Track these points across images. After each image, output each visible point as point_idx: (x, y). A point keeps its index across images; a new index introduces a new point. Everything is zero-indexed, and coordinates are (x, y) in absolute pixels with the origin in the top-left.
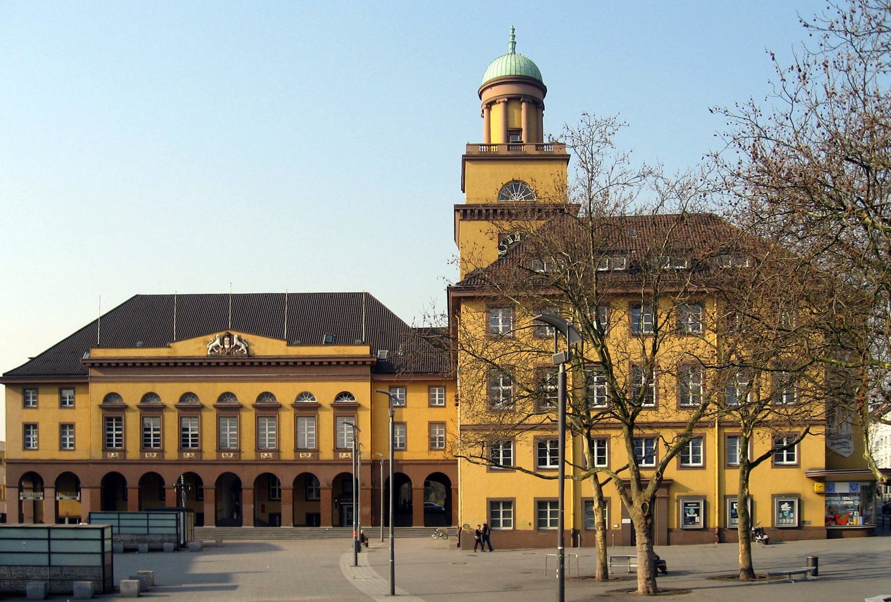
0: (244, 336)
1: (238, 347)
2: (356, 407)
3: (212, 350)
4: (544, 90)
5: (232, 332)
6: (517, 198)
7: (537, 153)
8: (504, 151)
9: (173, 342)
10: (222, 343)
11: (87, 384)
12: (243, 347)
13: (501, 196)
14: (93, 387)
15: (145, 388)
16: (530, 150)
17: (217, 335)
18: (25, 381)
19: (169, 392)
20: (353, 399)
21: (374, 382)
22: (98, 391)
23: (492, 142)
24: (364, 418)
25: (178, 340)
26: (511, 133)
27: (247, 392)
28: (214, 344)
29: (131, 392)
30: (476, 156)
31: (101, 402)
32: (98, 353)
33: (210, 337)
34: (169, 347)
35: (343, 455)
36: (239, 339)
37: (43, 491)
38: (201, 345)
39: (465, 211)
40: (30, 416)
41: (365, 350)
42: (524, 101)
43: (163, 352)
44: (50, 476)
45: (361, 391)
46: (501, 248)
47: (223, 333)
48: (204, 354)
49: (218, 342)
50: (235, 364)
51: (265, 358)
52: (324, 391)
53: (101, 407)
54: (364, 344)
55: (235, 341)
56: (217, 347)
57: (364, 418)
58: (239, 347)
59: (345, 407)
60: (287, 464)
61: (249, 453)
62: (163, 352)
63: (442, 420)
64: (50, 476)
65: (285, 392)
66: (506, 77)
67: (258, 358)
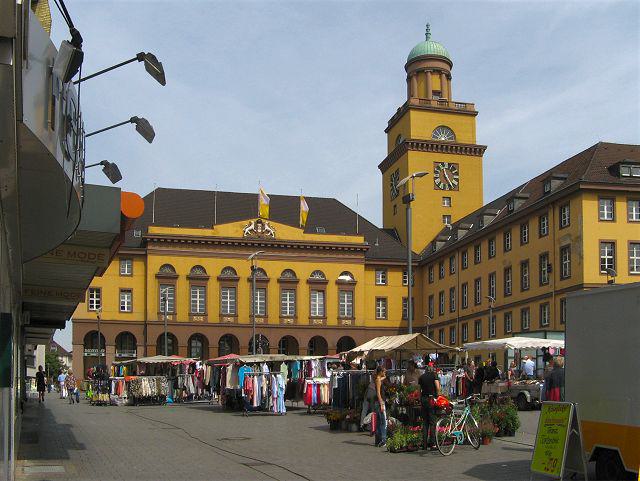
10: (256, 227)
11: (146, 256)
14: (151, 258)
15: (196, 261)
19: (214, 266)
21: (366, 265)
22: (155, 262)
25: (219, 223)
27: (274, 268)
29: (183, 265)
32: (154, 230)
33: (246, 223)
35: (226, 319)
41: (360, 240)
43: (208, 233)
44: (111, 335)
45: (358, 269)
47: (256, 220)
48: (240, 236)
49: (252, 227)
51: (289, 241)
52: (333, 271)
53: (157, 277)
54: (359, 234)
55: (267, 228)
62: (208, 233)
64: (111, 335)
65: (304, 270)
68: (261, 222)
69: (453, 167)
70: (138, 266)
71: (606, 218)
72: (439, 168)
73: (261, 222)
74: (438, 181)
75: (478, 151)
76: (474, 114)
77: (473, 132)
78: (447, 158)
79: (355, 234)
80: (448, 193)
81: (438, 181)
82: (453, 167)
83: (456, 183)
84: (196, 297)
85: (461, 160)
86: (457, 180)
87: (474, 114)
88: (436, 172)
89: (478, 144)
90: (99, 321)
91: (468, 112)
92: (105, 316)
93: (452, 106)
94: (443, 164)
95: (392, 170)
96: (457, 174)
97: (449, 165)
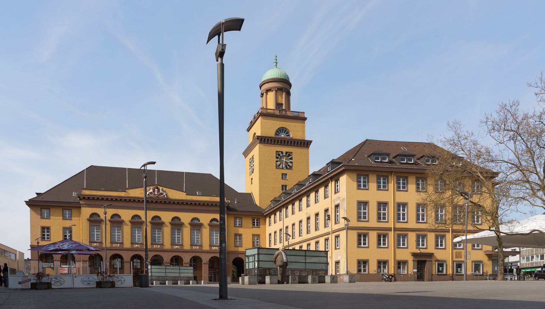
0: (165, 189)
1: (162, 194)
5: (159, 187)
9: (128, 189)
10: (154, 191)
11: (80, 207)
12: (165, 194)
13: (276, 134)
18: (38, 204)
20: (199, 221)
29: (106, 213)
30: (264, 114)
31: (88, 217)
34: (125, 192)
36: (163, 191)
37: (53, 262)
39: (261, 139)
40: (45, 223)
47: (153, 187)
49: (151, 191)
50: (161, 202)
53: (88, 220)
55: (161, 191)
56: (151, 193)
58: (162, 194)
60: (187, 252)
61: (187, 246)
62: (122, 194)
63: (258, 233)
66: (276, 79)
67: (172, 200)
68: (157, 188)
69: (289, 154)
71: (362, 187)
72: (279, 155)
73: (157, 188)
74: (279, 163)
75: (306, 144)
76: (305, 119)
77: (304, 131)
78: (284, 149)
80: (285, 171)
81: (279, 163)
82: (289, 154)
83: (291, 165)
85: (296, 151)
86: (291, 162)
87: (305, 119)
88: (277, 158)
89: (306, 139)
91: (300, 118)
93: (289, 114)
94: (282, 153)
95: (250, 156)
96: (291, 159)
97: (286, 153)
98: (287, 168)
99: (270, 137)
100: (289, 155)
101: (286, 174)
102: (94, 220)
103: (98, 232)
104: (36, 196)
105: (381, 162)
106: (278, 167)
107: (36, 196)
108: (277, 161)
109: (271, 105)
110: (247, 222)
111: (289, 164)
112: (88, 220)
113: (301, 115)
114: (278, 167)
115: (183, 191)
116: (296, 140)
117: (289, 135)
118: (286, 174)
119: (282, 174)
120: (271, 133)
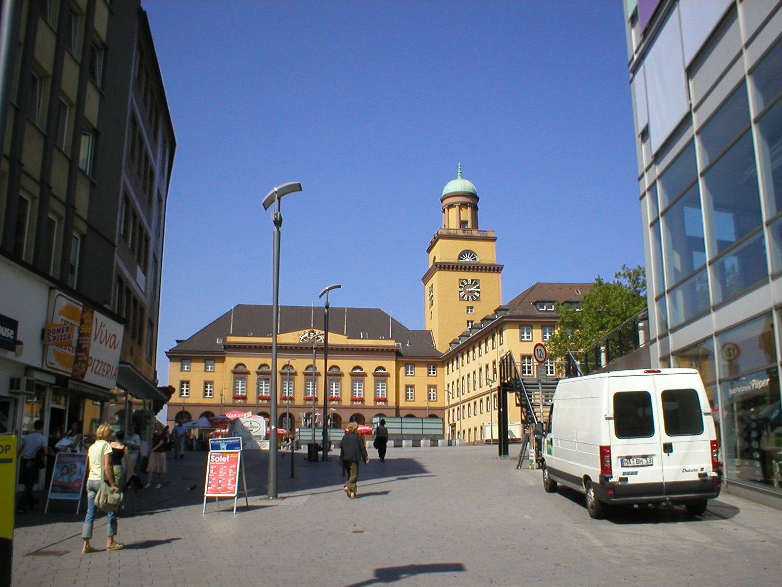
2: (387, 375)
3: (303, 340)
4: (478, 199)
5: (315, 330)
6: (467, 259)
7: (463, 234)
8: (460, 233)
10: (309, 335)
11: (224, 357)
13: (459, 258)
16: (475, 233)
17: (306, 331)
21: (396, 361)
22: (232, 361)
23: (450, 228)
24: (392, 381)
26: (463, 223)
28: (304, 336)
29: (252, 363)
33: (302, 332)
38: (296, 336)
41: (391, 343)
42: (469, 206)
45: (390, 365)
46: (460, 287)
47: (309, 330)
48: (297, 342)
49: (306, 335)
52: (369, 366)
56: (306, 338)
57: (392, 381)
59: (381, 376)
65: (346, 365)
68: (313, 332)
70: (218, 366)
72: (463, 283)
73: (313, 332)
78: (470, 276)
79: (387, 338)
80: (470, 303)
82: (475, 282)
84: (242, 389)
86: (478, 292)
90: (184, 405)
92: (191, 400)
94: (467, 280)
95: (429, 284)
96: (478, 288)
97: (472, 281)
98: (473, 300)
99: (452, 263)
100: (476, 284)
101: (472, 308)
102: (240, 373)
103: (244, 386)
104: (175, 345)
105: (546, 310)
106: (461, 299)
107: (175, 345)
108: (460, 292)
109: (454, 224)
110: (421, 371)
111: (476, 294)
112: (234, 373)
113: (490, 235)
114: (461, 299)
115: (343, 334)
116: (483, 265)
117: (475, 259)
118: (472, 308)
119: (468, 307)
120: (453, 258)
